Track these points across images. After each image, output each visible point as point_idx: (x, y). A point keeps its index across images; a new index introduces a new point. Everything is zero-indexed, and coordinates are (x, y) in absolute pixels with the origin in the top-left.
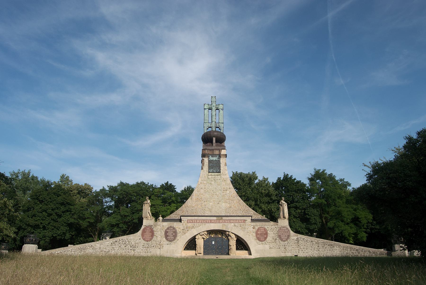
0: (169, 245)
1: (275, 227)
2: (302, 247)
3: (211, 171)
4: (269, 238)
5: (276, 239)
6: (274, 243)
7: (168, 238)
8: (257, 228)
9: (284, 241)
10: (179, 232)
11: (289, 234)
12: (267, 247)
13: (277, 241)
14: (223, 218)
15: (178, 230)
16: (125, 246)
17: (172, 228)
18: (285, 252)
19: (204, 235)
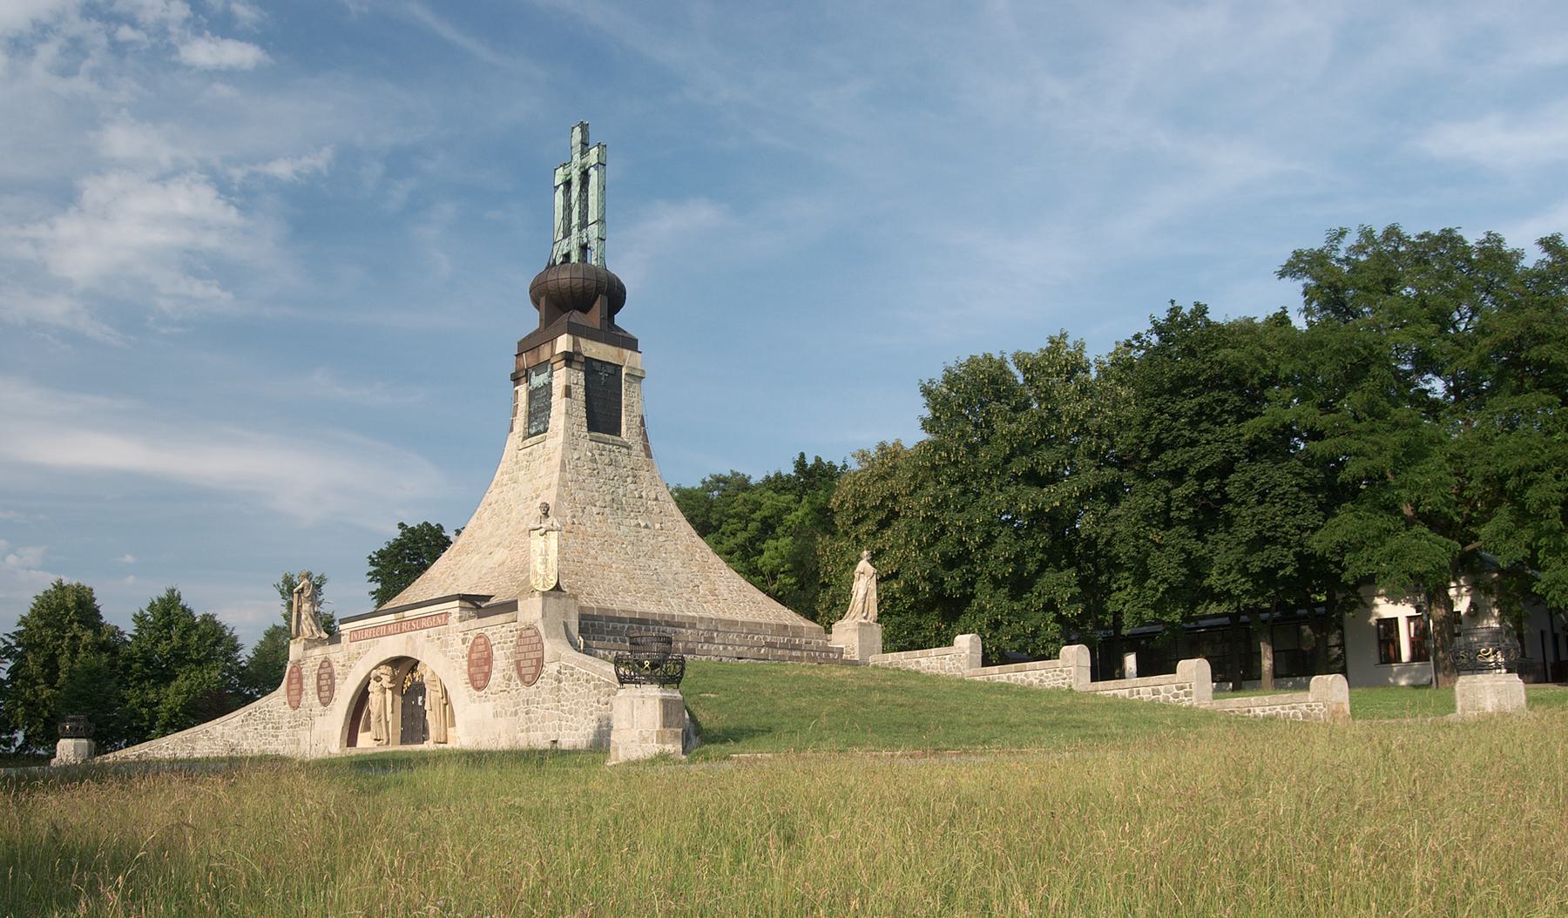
0: (322, 717)
1: (511, 631)
2: (567, 706)
3: (533, 431)
4: (496, 677)
5: (509, 680)
6: (506, 693)
7: (322, 694)
8: (471, 637)
9: (528, 683)
10: (339, 674)
11: (538, 655)
12: (489, 707)
13: (513, 684)
14: (407, 613)
15: (337, 668)
16: (265, 728)
17: (326, 664)
18: (528, 730)
19: (382, 676)
